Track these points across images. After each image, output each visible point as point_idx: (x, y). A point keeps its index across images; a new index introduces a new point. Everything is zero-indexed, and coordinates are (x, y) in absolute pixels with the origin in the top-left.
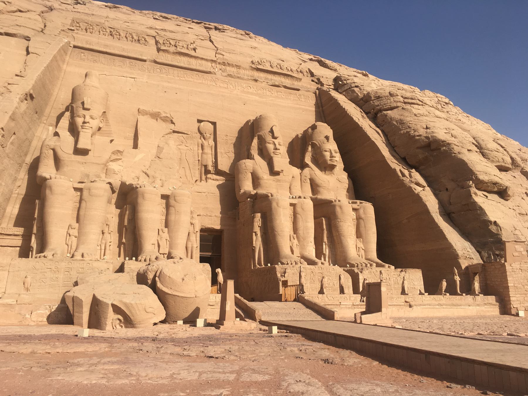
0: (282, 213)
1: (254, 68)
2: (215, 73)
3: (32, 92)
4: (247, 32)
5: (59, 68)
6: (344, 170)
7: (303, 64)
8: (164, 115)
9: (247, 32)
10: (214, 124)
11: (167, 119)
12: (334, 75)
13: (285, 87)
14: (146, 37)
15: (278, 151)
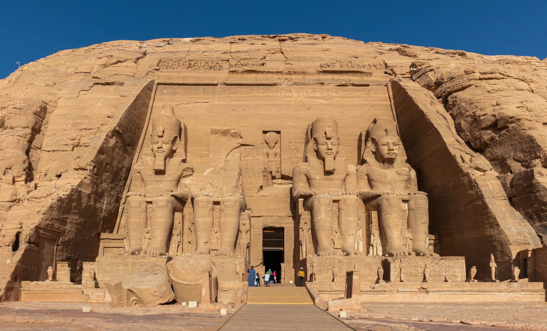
0: (323, 210)
1: (321, 72)
2: (281, 84)
3: (117, 128)
4: (324, 35)
5: (146, 105)
6: (408, 161)
7: (379, 56)
8: (233, 131)
9: (324, 35)
10: (278, 132)
11: (237, 135)
12: (410, 61)
13: (354, 85)
14: (220, 63)
15: (330, 151)
